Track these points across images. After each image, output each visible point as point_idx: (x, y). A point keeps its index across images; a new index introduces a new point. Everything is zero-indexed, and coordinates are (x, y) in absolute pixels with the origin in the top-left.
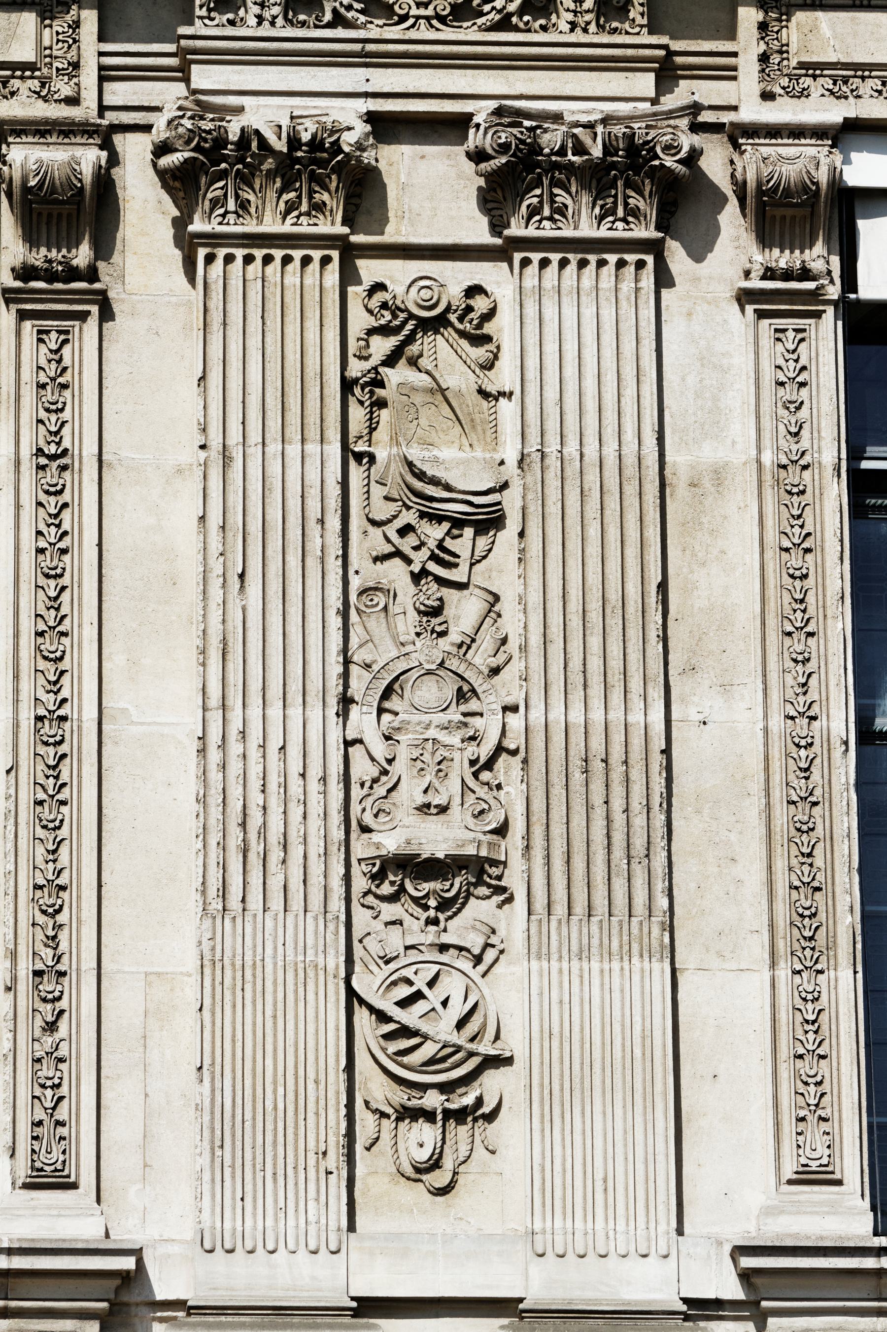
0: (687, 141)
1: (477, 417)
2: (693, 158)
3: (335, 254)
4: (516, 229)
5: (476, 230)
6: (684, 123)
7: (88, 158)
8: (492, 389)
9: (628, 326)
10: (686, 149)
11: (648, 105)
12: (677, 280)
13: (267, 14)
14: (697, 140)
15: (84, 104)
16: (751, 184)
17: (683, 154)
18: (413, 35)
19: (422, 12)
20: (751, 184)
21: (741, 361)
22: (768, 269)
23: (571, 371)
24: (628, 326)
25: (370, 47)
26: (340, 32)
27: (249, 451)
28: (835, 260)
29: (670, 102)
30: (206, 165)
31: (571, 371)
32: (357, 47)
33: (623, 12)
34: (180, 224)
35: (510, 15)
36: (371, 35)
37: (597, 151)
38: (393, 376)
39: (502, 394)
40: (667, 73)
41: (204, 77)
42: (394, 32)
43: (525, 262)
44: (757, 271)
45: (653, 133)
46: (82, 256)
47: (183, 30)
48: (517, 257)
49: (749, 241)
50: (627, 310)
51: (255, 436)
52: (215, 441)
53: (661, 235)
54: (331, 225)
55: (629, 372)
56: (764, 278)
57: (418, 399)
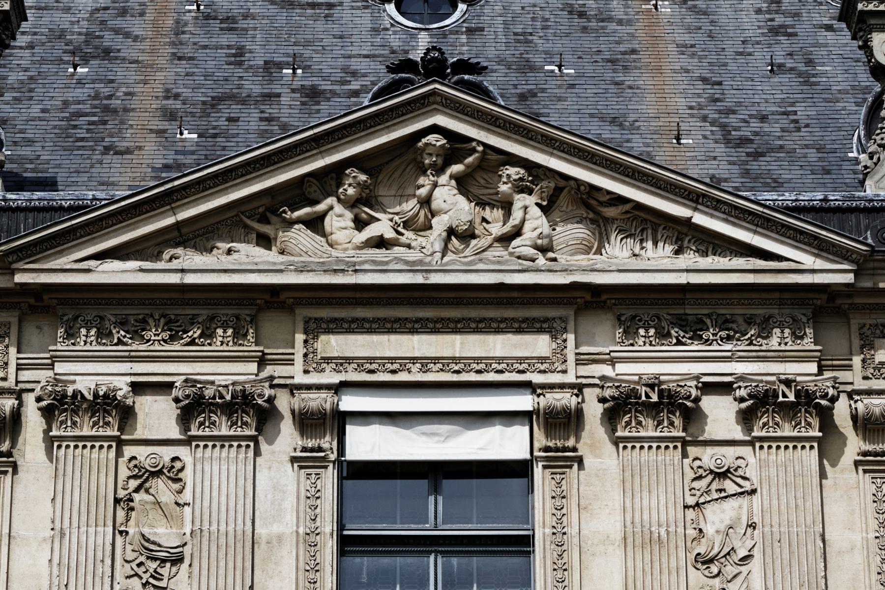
0: (268, 392)
1: (174, 514)
6: (267, 384)
8: (181, 502)
9: (241, 474)
11: (254, 377)
12: (263, 453)
14: (272, 392)
15: (9, 380)
16: (297, 411)
17: (266, 398)
18: (152, 348)
19: (157, 338)
20: (297, 411)
21: (292, 488)
22: (303, 447)
23: (215, 493)
24: (241, 474)
25: (133, 354)
26: (120, 348)
27: (72, 531)
29: (264, 374)
31: (215, 493)
32: (127, 354)
33: (245, 335)
35: (195, 339)
36: (133, 348)
37: (228, 397)
38: (137, 497)
39: (185, 504)
40: (262, 362)
41: (60, 368)
42: (143, 347)
44: (299, 448)
45: (254, 389)
49: (296, 434)
50: (241, 466)
51: (75, 524)
52: (58, 526)
55: (241, 493)
56: (302, 451)
57: (148, 507)
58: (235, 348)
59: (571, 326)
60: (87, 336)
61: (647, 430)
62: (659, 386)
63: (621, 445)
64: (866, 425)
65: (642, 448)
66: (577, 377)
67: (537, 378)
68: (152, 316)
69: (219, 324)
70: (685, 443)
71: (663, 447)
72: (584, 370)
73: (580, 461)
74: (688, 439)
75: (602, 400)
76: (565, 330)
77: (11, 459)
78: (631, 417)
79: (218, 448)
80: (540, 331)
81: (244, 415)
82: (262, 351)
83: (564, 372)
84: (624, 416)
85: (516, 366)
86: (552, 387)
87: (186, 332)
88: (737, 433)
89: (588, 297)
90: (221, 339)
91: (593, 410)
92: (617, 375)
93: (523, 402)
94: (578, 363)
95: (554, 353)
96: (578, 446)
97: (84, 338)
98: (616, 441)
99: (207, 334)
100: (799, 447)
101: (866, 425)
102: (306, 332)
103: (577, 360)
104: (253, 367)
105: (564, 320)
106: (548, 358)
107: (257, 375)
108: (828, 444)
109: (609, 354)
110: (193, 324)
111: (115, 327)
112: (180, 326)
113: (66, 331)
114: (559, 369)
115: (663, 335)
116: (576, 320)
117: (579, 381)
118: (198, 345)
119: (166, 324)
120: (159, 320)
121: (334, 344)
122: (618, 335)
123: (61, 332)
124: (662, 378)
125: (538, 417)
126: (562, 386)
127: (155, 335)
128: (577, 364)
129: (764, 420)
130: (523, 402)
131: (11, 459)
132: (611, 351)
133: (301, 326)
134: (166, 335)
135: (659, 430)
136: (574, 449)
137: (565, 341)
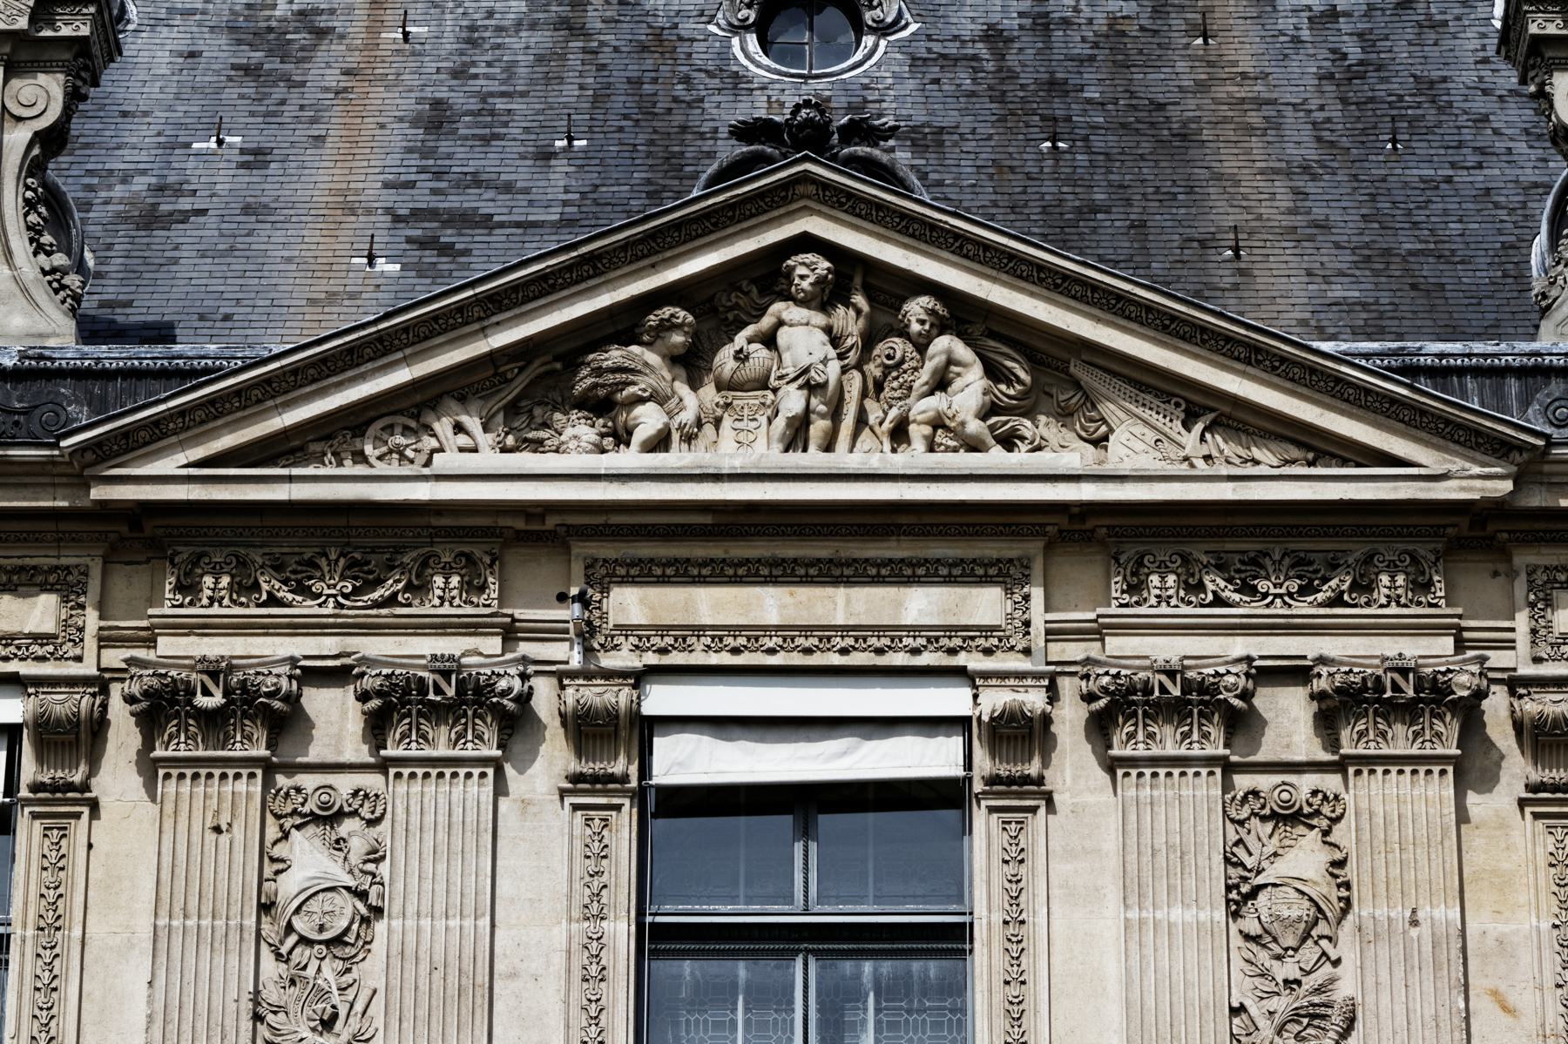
2: (525, 699)
5: (363, 754)
7: (84, 702)
28: (633, 770)
30: (162, 708)
33: (482, 588)
37: (451, 692)
46: (77, 777)
53: (499, 753)
54: (261, 751)
60: (213, 590)
61: (435, 747)
62: (459, 673)
63: (1120, 772)
64: (1541, 738)
65: (469, 776)
67: (974, 662)
68: (325, 555)
70: (269, 769)
71: (462, 775)
74: (1234, 758)
75: (1089, 698)
76: (1026, 579)
77: (88, 795)
78: (410, 724)
79: (174, 780)
80: (985, 581)
81: (247, 722)
82: (512, 616)
84: (400, 721)
85: (800, 641)
90: (209, 593)
91: (1070, 718)
93: (951, 700)
94: (1052, 634)
95: (1010, 617)
96: (1047, 773)
97: (209, 593)
98: (1112, 766)
100: (448, 776)
101: (1541, 738)
110: (392, 568)
113: (178, 580)
119: (348, 567)
120: (337, 561)
121: (629, 604)
123: (171, 580)
124: (235, 662)
129: (1128, 729)
130: (951, 700)
131: (88, 795)
133: (578, 569)
135: (172, 747)
136: (1040, 780)
137: (1027, 598)
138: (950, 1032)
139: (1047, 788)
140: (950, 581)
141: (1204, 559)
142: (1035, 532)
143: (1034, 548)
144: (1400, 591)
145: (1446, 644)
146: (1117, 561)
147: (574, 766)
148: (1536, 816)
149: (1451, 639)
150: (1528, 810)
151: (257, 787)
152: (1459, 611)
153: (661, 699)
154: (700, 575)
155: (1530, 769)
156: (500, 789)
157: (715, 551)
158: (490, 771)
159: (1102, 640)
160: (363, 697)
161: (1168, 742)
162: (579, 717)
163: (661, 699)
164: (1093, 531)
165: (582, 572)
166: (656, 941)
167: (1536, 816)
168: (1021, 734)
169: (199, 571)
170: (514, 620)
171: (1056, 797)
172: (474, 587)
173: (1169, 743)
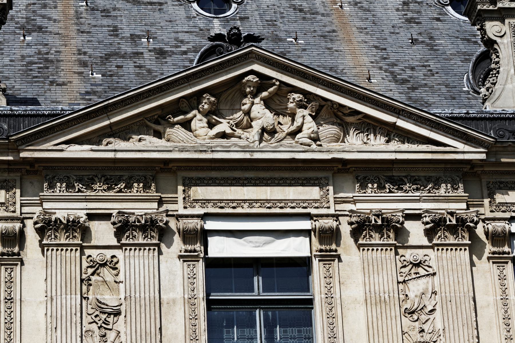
0: (165, 219)
2: (167, 223)
3: (79, 248)
4: (124, 241)
5: (114, 242)
6: (164, 214)
7: (18, 226)
10: (165, 221)
13: (62, 190)
14: (168, 219)
17: (164, 222)
26: (80, 194)
28: (202, 248)
30: (47, 227)
32: (84, 197)
33: (149, 188)
34: (40, 241)
36: (87, 194)
37: (143, 222)
40: (161, 202)
41: (46, 205)
42: (93, 194)
43: (126, 249)
47: (41, 194)
48: (124, 248)
58: (145, 194)
59: (331, 182)
66: (336, 211)
69: (135, 181)
72: (339, 207)
73: (339, 257)
74: (397, 244)
75: (351, 224)
76: (328, 185)
80: (314, 185)
82: (160, 196)
83: (329, 208)
86: (322, 216)
87: (116, 185)
88: (425, 241)
89: (340, 166)
92: (357, 209)
93: (306, 225)
95: (322, 197)
99: (129, 186)
102: (184, 185)
103: (335, 201)
104: (155, 205)
105: (327, 178)
106: (319, 200)
107: (157, 209)
108: (475, 247)
109: (352, 198)
110: (120, 180)
111: (76, 183)
112: (113, 182)
114: (325, 206)
115: (381, 187)
116: (333, 179)
117: (337, 213)
118: (123, 192)
119: (105, 181)
120: (101, 178)
121: (200, 192)
122: (357, 188)
125: (315, 233)
126: (327, 216)
127: (99, 187)
128: (335, 204)
130: (306, 225)
132: (354, 196)
133: (181, 182)
134: (105, 187)
137: (328, 190)
138: (304, 333)
139: (338, 253)
140: (303, 185)
141: (75, 178)
142: (330, 169)
143: (329, 174)
144: (375, 189)
145: (464, 206)
146: (357, 179)
147: (184, 247)
148: (493, 263)
149: (465, 204)
150: (491, 261)
151: (78, 253)
152: (467, 195)
153: (210, 225)
154: (302, 183)
155: (491, 247)
156: (160, 253)
157: (286, 175)
158: (157, 248)
159: (355, 204)
160: (114, 224)
161: (376, 239)
162: (184, 231)
163: (210, 225)
164: (349, 169)
165: (182, 182)
166: (210, 304)
167: (493, 263)
168: (330, 236)
169: (55, 182)
170: (161, 198)
171: (342, 257)
172: (147, 187)
173: (62, 239)
